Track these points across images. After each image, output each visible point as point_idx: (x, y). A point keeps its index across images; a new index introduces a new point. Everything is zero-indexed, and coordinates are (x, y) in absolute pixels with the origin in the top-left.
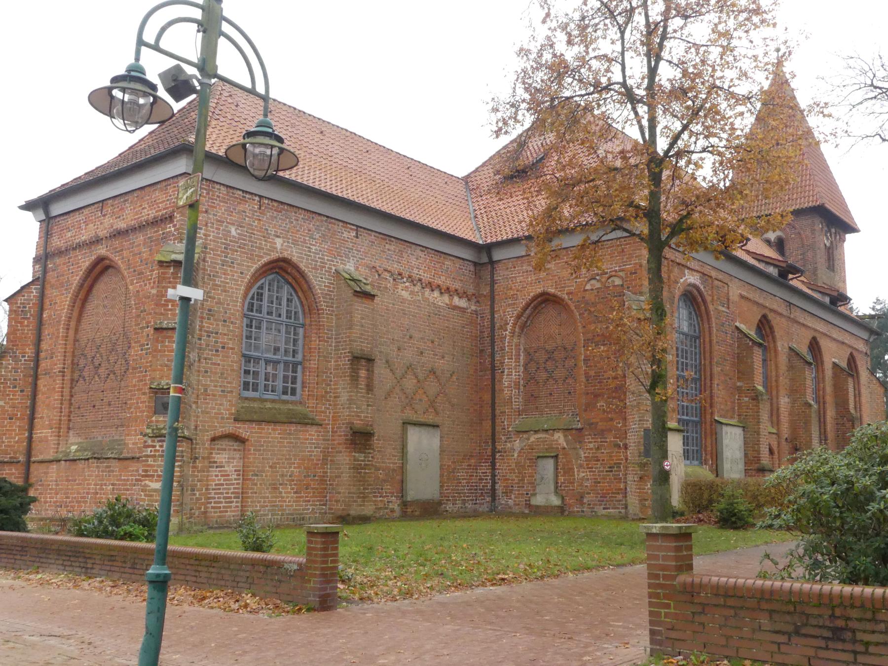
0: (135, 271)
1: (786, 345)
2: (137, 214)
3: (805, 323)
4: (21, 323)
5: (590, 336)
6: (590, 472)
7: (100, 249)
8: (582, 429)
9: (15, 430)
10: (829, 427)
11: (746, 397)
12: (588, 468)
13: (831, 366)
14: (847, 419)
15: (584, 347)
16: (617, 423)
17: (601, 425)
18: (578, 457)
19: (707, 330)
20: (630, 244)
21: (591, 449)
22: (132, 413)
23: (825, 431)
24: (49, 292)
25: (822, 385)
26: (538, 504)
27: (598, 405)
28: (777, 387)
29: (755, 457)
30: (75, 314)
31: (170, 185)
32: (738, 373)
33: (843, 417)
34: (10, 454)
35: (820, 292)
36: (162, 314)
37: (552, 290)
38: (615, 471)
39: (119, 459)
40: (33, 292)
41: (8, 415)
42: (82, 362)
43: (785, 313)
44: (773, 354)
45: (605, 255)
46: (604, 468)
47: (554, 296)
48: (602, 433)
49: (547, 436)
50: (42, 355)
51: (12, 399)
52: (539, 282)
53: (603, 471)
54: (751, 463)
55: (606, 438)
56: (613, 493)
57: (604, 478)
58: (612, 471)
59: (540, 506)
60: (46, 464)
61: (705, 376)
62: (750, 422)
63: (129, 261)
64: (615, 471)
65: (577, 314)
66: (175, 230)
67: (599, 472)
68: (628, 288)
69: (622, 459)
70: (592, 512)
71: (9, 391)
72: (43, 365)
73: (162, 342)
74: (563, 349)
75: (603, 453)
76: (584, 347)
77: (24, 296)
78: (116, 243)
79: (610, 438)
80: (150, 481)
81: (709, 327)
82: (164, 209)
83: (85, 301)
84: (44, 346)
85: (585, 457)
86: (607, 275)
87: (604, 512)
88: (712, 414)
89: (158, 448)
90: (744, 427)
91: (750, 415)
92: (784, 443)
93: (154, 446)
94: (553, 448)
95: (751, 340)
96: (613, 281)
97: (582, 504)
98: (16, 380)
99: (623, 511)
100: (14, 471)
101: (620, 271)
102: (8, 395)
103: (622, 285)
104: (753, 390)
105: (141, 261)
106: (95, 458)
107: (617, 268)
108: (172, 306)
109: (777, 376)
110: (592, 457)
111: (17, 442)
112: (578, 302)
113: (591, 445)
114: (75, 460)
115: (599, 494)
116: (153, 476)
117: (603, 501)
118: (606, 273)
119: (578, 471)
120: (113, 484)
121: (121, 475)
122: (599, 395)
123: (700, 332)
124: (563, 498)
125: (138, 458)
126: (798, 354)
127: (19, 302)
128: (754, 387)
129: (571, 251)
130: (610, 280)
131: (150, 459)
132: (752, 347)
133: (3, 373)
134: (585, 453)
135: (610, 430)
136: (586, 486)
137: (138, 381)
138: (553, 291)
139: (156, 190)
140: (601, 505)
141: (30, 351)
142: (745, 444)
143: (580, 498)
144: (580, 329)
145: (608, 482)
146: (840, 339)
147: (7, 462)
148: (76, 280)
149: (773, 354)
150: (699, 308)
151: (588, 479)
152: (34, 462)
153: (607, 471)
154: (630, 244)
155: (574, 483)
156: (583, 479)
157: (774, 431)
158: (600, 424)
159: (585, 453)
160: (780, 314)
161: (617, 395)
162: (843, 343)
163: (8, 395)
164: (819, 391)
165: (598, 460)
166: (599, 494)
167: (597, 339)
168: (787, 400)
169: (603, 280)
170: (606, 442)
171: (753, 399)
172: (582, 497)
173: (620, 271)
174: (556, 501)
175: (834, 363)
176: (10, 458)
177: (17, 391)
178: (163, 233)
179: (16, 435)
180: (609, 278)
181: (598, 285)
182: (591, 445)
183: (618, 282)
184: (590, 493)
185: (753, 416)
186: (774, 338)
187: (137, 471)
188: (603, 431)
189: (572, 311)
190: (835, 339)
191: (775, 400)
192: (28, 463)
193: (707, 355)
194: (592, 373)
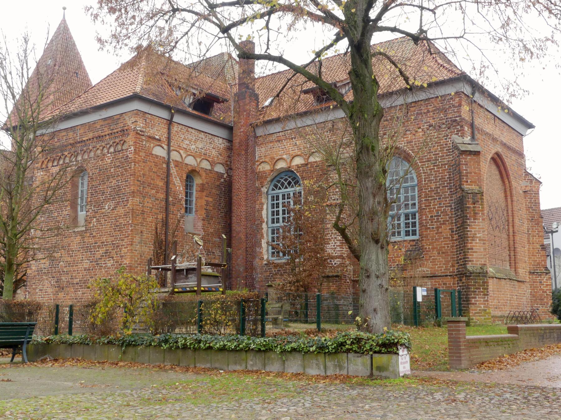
120: (516, 295)
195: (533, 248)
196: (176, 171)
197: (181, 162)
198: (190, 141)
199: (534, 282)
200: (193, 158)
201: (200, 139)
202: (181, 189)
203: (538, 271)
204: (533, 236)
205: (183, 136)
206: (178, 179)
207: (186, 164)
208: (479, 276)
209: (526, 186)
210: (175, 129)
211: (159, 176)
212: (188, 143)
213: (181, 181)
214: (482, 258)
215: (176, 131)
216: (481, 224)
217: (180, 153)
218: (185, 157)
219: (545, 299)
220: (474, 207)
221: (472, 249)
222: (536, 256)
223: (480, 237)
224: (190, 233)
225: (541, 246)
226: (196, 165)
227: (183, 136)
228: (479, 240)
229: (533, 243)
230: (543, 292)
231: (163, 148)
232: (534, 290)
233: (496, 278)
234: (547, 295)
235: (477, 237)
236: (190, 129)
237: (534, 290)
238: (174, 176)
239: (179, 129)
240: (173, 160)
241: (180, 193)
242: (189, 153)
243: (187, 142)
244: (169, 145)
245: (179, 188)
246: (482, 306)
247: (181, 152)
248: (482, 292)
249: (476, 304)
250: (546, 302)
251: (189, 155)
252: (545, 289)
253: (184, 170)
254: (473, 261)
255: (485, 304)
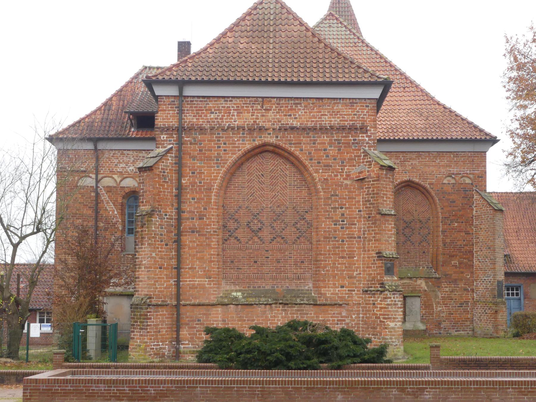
0: (319, 163)
2: (314, 117)
4: (163, 186)
5: (447, 215)
6: (445, 307)
7: (264, 137)
8: (440, 278)
9: (163, 278)
12: (444, 304)
15: (442, 222)
16: (466, 275)
17: (454, 276)
18: (436, 296)
20: (478, 157)
21: (447, 292)
22: (327, 271)
24: (188, 162)
26: (407, 329)
27: (453, 262)
30: (225, 184)
31: (357, 103)
34: (161, 298)
36: (382, 204)
37: (417, 180)
38: (465, 307)
39: (315, 305)
40: (169, 159)
41: (159, 265)
42: (232, 225)
45: (459, 162)
46: (456, 304)
47: (417, 184)
48: (455, 281)
49: (411, 282)
50: (185, 215)
51: (160, 252)
52: (405, 173)
53: (455, 307)
55: (458, 285)
56: (462, 321)
57: (455, 312)
58: (462, 307)
59: (410, 330)
60: (205, 307)
63: (310, 153)
64: (465, 307)
65: (437, 199)
66: (369, 140)
67: (452, 307)
68: (476, 186)
69: (470, 299)
70: (447, 333)
71: (159, 245)
72: (186, 225)
73: (385, 224)
74: (418, 222)
75: (456, 294)
76: (442, 222)
77: (163, 162)
78: (291, 137)
79: (462, 285)
80: (390, 322)
82: (351, 121)
83: (233, 174)
84: (186, 207)
85: (442, 297)
86: (460, 176)
87: (456, 333)
89: (392, 299)
93: (390, 298)
94: (416, 290)
96: (464, 180)
97: (440, 328)
98: (161, 235)
99: (470, 332)
100: (165, 312)
101: (470, 174)
102: (158, 248)
103: (472, 184)
105: (327, 156)
106: (280, 304)
107: (468, 172)
108: (386, 198)
110: (447, 297)
111: (165, 288)
112: (438, 191)
113: (447, 289)
114: (252, 305)
115: (452, 321)
116: (390, 318)
117: (455, 326)
118: (460, 174)
119: (437, 306)
121: (318, 317)
122: (453, 256)
124: (427, 326)
125: (341, 305)
127: (160, 167)
129: (432, 154)
130: (462, 179)
131: (390, 307)
133: (153, 229)
134: (442, 294)
135: (461, 280)
136: (443, 316)
137: (333, 248)
138: (417, 180)
139: (338, 103)
140: (453, 329)
141: (172, 212)
143: (438, 324)
144: (439, 210)
145: (459, 314)
147: (160, 305)
148: (232, 158)
151: (444, 312)
152: (185, 305)
153: (458, 307)
154: (478, 157)
155: (433, 314)
156: (440, 311)
158: (453, 275)
159: (442, 294)
161: (467, 257)
163: (158, 248)
165: (452, 299)
166: (452, 321)
167: (452, 218)
169: (457, 178)
170: (458, 287)
172: (440, 324)
173: (470, 174)
174: (422, 327)
176: (162, 301)
177: (163, 245)
178: (355, 140)
179: (165, 282)
180: (462, 177)
181: (453, 181)
182: (447, 289)
183: (468, 181)
184: (445, 321)
187: (340, 314)
188: (456, 280)
189: (432, 197)
192: (177, 306)
194: (448, 241)
195: (368, 257)
196: (109, 196)
197: (114, 187)
198: (127, 163)
199: (366, 304)
200: (131, 179)
201: (141, 158)
202: (116, 213)
203: (373, 289)
204: (369, 241)
205: (116, 161)
206: (111, 204)
207: (123, 188)
208: (137, 308)
209: (361, 172)
210: (106, 155)
211: (87, 205)
212: (124, 165)
213: (114, 205)
214: (145, 288)
215: (107, 158)
216: (146, 249)
217: (113, 178)
218: (121, 181)
219: (378, 327)
220: (142, 231)
221: (139, 278)
222: (371, 267)
223: (145, 264)
224: (129, 255)
225: (377, 253)
226: (136, 185)
227: (116, 161)
228: (144, 268)
229: (369, 251)
230: (376, 318)
231: (91, 177)
232: (366, 314)
233: (241, 305)
234: (381, 321)
235: (142, 265)
236: (125, 152)
237: (366, 314)
238: (105, 202)
239: (112, 155)
240: (104, 187)
241: (114, 217)
242: (125, 176)
243: (123, 165)
244: (97, 174)
245: (113, 211)
246: (139, 341)
247: (115, 177)
248: (139, 325)
249: (134, 338)
250: (379, 332)
251: (126, 177)
252: (378, 313)
253: (119, 194)
254: (139, 291)
255: (140, 339)
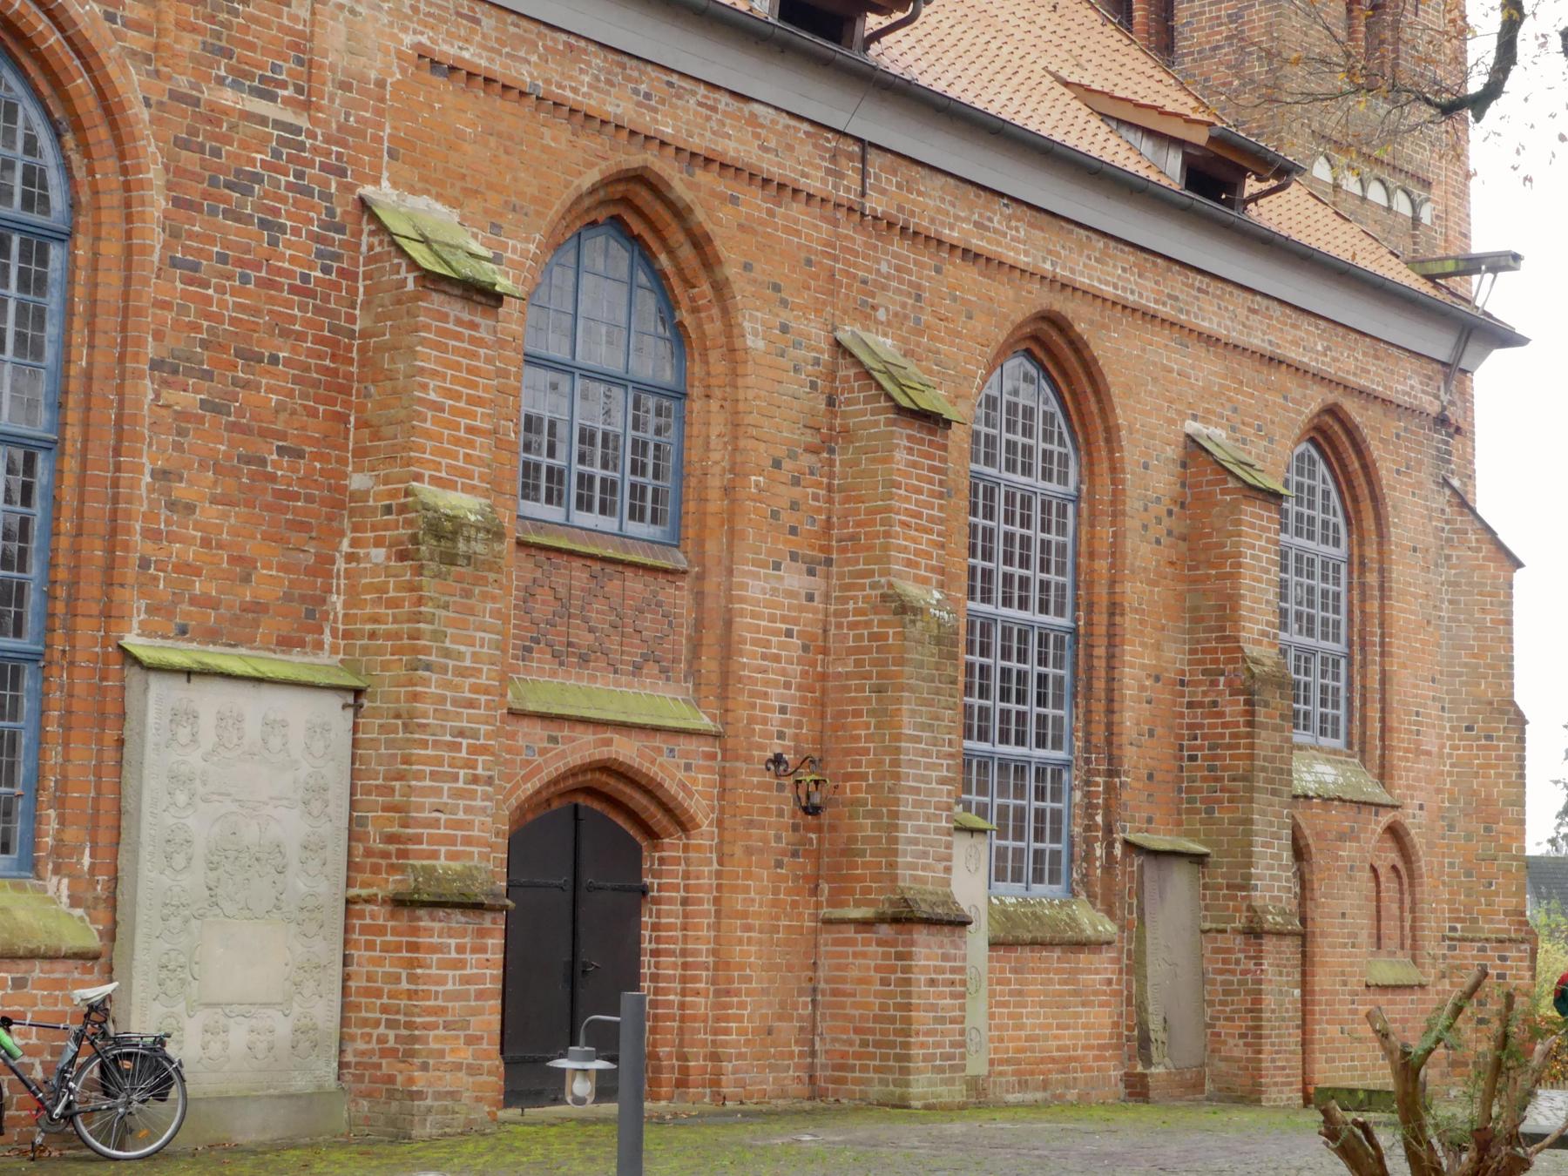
1: (815, 332)
3: (977, 243)
10: (1130, 718)
11: (378, 543)
13: (1172, 452)
14: (1229, 684)
19: (112, 199)
23: (1109, 742)
25: (1105, 532)
28: (730, 517)
29: (391, 839)
32: (362, 424)
33: (1213, 675)
35: (1149, 133)
43: (815, 183)
44: (718, 366)
54: (376, 869)
61: (86, 424)
62: (385, 666)
81: (127, 187)
88: (110, 615)
90: (358, 692)
91: (389, 636)
92: (752, 777)
95: (413, 265)
104: (403, 509)
109: (736, 471)
123: (74, 206)
126: (867, 374)
128: (407, 493)
132: (416, 298)
142: (355, 774)
146: (1256, 341)
149: (718, 366)
150: (57, 84)
157: (704, 722)
160: (783, 189)
162: (1273, 361)
164: (1092, 556)
168: (794, 579)
171: (402, 556)
175: (1194, 447)
185: (397, 636)
186: (721, 289)
190: (1210, 340)
191: (713, 583)
193: (108, 322)
